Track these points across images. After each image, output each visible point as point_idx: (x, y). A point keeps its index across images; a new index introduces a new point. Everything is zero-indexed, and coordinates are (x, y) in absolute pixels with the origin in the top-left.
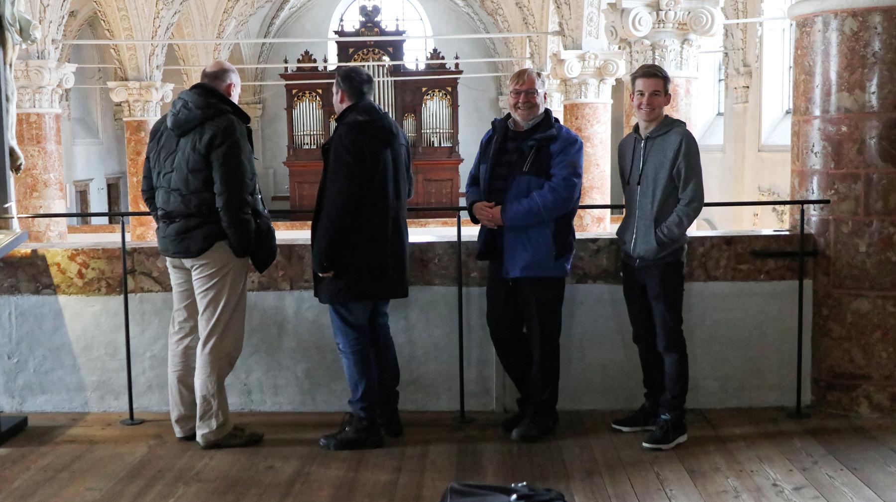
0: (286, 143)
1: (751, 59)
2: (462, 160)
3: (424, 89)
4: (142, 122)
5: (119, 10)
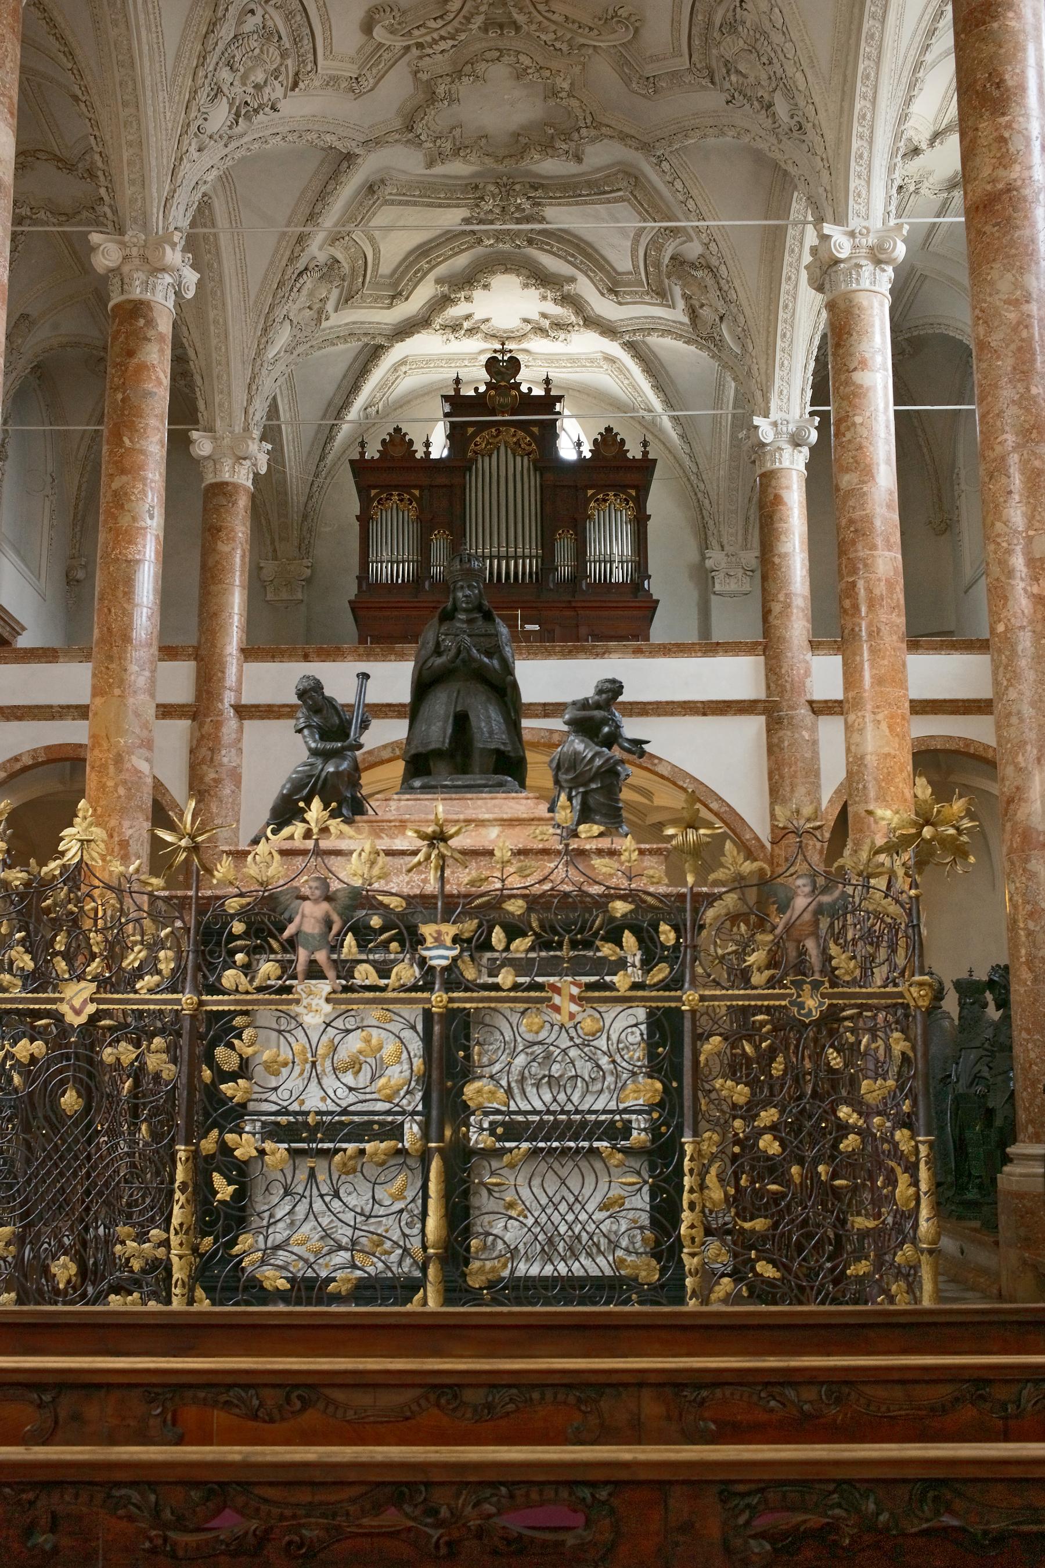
0: (356, 571)
2: (657, 601)
3: (590, 492)
4: (141, 302)
5: (125, 104)
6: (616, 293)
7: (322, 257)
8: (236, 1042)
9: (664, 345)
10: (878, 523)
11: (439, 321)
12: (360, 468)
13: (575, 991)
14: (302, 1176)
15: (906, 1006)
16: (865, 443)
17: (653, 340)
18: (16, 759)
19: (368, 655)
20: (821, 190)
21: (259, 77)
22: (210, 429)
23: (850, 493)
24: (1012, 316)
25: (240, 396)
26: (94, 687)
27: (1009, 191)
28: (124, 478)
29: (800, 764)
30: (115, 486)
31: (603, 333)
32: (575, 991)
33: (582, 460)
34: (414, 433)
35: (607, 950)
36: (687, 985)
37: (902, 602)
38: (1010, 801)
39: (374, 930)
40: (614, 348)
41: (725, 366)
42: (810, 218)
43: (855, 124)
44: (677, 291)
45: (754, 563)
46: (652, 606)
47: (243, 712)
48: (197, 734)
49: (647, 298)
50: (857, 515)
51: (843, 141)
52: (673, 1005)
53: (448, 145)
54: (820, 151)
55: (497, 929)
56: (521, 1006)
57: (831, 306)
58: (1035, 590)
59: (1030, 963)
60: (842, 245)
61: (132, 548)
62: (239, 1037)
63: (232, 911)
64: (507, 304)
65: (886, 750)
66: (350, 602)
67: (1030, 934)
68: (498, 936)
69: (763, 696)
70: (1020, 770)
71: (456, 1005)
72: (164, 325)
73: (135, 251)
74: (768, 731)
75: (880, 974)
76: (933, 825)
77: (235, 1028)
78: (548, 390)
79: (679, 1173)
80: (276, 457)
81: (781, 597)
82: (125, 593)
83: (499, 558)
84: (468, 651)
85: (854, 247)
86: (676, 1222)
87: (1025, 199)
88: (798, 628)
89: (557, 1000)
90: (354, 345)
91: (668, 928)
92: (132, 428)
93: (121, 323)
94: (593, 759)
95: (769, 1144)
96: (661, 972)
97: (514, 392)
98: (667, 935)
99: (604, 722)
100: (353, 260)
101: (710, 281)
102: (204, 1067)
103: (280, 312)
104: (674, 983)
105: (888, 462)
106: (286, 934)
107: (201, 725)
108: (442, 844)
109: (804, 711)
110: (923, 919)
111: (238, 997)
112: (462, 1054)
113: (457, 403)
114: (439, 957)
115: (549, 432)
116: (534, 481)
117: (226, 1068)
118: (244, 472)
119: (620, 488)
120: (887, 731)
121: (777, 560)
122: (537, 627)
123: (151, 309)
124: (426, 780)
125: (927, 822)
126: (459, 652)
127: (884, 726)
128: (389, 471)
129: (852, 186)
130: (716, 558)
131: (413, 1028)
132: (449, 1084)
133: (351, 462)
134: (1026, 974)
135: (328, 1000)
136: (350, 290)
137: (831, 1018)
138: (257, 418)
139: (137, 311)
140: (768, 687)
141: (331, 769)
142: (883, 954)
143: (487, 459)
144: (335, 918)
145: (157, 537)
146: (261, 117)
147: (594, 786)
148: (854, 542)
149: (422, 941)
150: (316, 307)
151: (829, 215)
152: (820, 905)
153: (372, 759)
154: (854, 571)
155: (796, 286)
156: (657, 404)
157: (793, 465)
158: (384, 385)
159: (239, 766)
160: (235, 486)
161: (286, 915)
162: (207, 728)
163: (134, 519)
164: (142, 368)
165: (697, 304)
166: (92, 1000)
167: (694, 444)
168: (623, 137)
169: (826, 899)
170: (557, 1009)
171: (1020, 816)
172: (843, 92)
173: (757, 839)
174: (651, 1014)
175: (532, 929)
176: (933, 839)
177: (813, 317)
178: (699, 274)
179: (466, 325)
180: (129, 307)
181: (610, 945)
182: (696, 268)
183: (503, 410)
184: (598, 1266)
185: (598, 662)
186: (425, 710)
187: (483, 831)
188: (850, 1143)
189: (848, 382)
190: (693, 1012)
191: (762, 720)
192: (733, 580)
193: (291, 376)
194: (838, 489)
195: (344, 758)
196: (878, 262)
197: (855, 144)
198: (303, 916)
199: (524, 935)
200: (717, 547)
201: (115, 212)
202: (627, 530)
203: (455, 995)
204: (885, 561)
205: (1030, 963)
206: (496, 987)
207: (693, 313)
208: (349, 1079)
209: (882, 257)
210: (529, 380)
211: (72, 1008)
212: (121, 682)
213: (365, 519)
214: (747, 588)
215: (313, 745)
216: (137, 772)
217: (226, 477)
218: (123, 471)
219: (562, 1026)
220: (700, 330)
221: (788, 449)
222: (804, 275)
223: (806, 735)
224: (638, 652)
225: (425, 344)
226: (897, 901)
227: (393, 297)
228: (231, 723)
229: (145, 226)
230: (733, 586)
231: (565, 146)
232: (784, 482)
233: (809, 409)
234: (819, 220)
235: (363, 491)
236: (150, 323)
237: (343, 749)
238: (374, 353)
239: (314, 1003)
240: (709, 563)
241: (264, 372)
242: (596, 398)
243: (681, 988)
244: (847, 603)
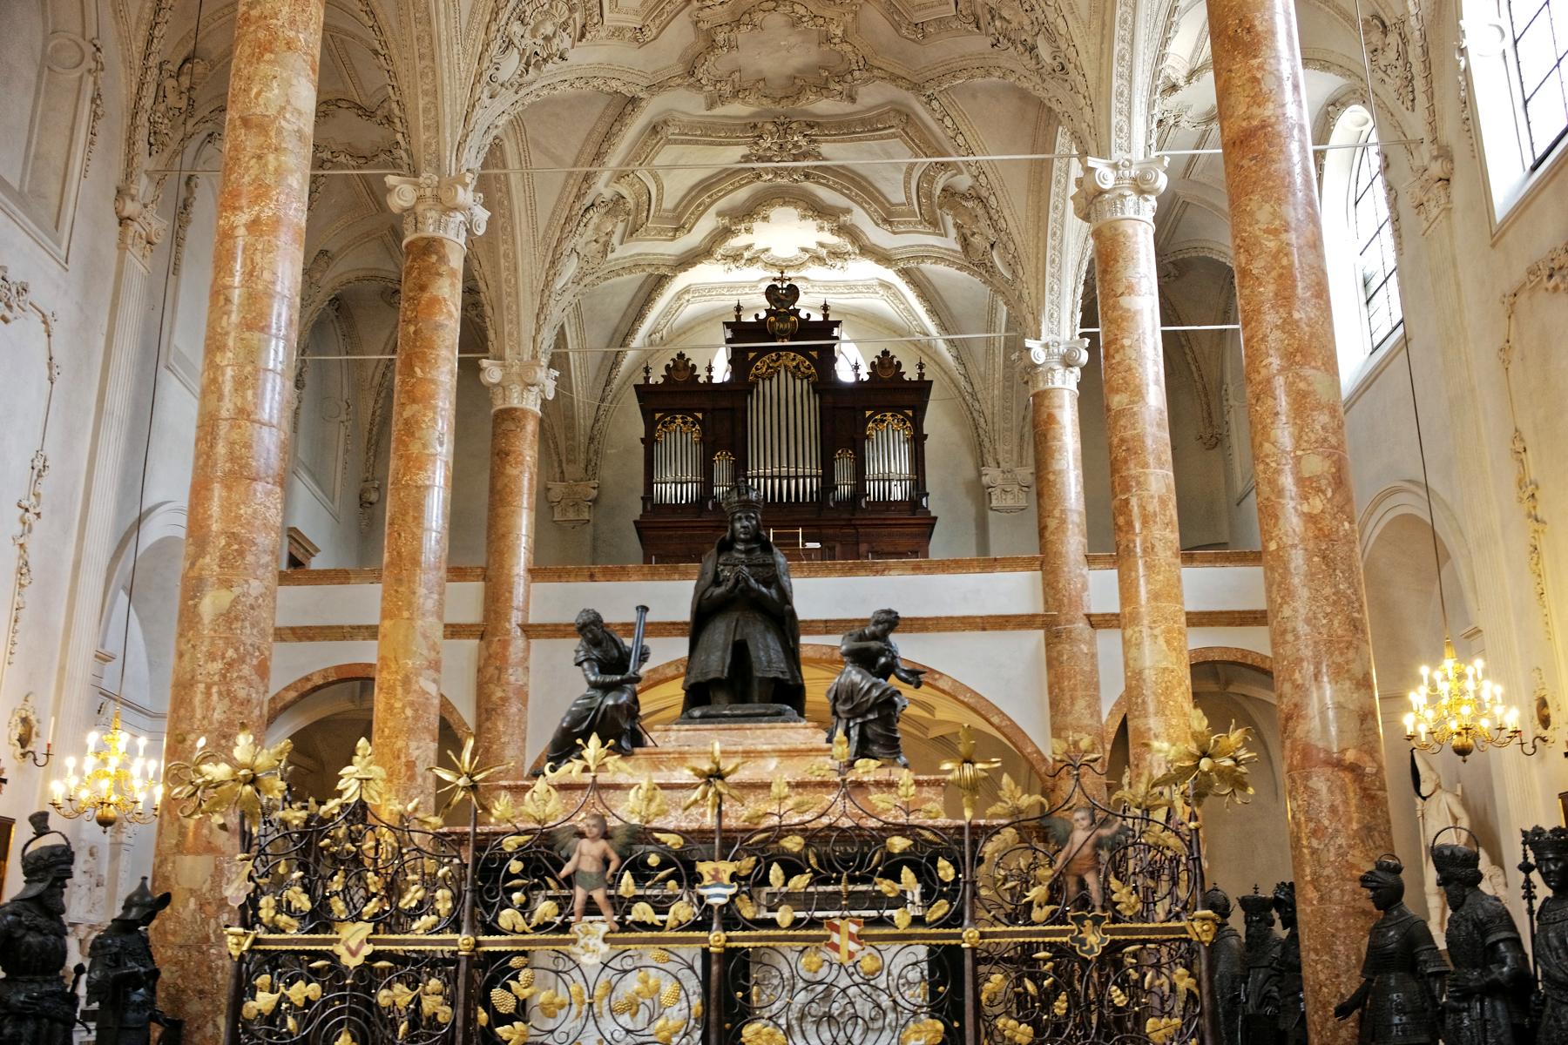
1: (1449, 131)
2: (935, 518)
3: (868, 413)
4: (434, 240)
5: (422, 57)
6: (891, 223)
7: (608, 194)
8: (512, 983)
9: (937, 271)
10: (1149, 441)
11: (720, 251)
12: (645, 393)
13: (854, 929)
15: (1189, 941)
16: (1134, 365)
17: (928, 267)
18: (307, 679)
19: (653, 575)
20: (1084, 125)
21: (548, 29)
22: (500, 357)
23: (1121, 413)
24: (1271, 244)
25: (528, 325)
26: (383, 610)
27: (1263, 127)
28: (415, 407)
29: (1079, 677)
30: (406, 414)
31: (878, 261)
32: (854, 929)
33: (859, 383)
34: (697, 358)
35: (885, 886)
36: (966, 922)
37: (1175, 518)
38: (1289, 718)
39: (652, 868)
40: (890, 275)
41: (997, 291)
42: (1075, 152)
43: (1115, 65)
44: (949, 220)
45: (1030, 479)
47: (529, 631)
48: (485, 654)
49: (920, 228)
50: (1129, 434)
51: (1104, 79)
52: (953, 942)
53: (728, 88)
54: (1082, 90)
55: (775, 866)
56: (800, 945)
57: (1097, 234)
58: (1306, 508)
59: (1315, 882)
60: (1106, 177)
61: (422, 475)
62: (515, 978)
63: (509, 850)
64: (785, 235)
65: (1164, 664)
66: (635, 522)
67: (1314, 852)
68: (776, 872)
69: (1040, 610)
70: (1297, 687)
71: (734, 945)
72: (456, 261)
73: (428, 192)
74: (1047, 645)
75: (1161, 910)
76: (1210, 756)
77: (512, 969)
78: (826, 316)
80: (563, 383)
81: (1057, 513)
82: (415, 518)
83: (780, 478)
84: (746, 581)
85: (1118, 179)
87: (1279, 135)
88: (1073, 542)
89: (836, 938)
90: (639, 276)
91: (946, 863)
92: (424, 360)
93: (414, 260)
94: (869, 690)
96: (941, 908)
97: (793, 319)
98: (945, 870)
99: (881, 652)
100: (638, 196)
101: (980, 211)
102: (480, 1009)
103: (567, 246)
104: (955, 919)
105: (1157, 382)
106: (564, 873)
107: (489, 645)
108: (719, 782)
109: (1081, 625)
110: (1203, 852)
111: (515, 937)
112: (740, 994)
113: (739, 330)
114: (717, 895)
115: (827, 357)
116: (813, 403)
117: (502, 1010)
118: (532, 398)
119: (897, 409)
120: (1164, 647)
121: (1051, 477)
122: (817, 545)
123: (443, 246)
124: (705, 709)
125: (1205, 754)
126: (737, 581)
127: (1161, 640)
128: (673, 395)
129: (1114, 122)
130: (992, 475)
131: (691, 968)
132: (728, 1026)
133: (636, 386)
134: (1312, 894)
135: (605, 940)
136: (635, 223)
138: (545, 346)
139: (430, 248)
140: (1046, 602)
141: (610, 702)
142: (1164, 887)
143: (767, 383)
144: (613, 856)
145: (447, 463)
146: (550, 65)
147: (871, 717)
148: (1126, 461)
149: (698, 878)
150: (602, 240)
151: (1092, 147)
152: (1100, 839)
153: (656, 677)
154: (1127, 489)
155: (1063, 215)
157: (1065, 384)
159: (526, 684)
160: (524, 412)
161: (563, 853)
162: (495, 647)
163: (425, 446)
164: (435, 301)
165: (968, 233)
166: (368, 941)
167: (969, 366)
168: (894, 78)
169: (1105, 832)
170: (836, 948)
171: (1300, 733)
172: (1103, 36)
173: (1038, 752)
174: (931, 952)
175: (810, 866)
176: (1211, 770)
177: (1080, 244)
178: (970, 204)
179: (747, 255)
180: (422, 244)
181: (889, 881)
182: (967, 199)
183: (782, 334)
185: (878, 578)
186: (705, 639)
187: (761, 762)
189: (1115, 307)
190: (974, 949)
191: (1041, 633)
192: (1009, 496)
193: (578, 306)
194: (1109, 410)
195: (623, 691)
196: (1141, 192)
197: (1116, 83)
198: (581, 854)
199: (803, 872)
200: (993, 464)
201: (410, 155)
202: (905, 449)
203: (733, 934)
204: (1156, 480)
205: (1315, 882)
206: (772, 924)
207: (965, 242)
208: (625, 1019)
209: (1145, 187)
210: (808, 307)
211: (349, 949)
212: (410, 605)
213: (649, 442)
214: (1023, 503)
215: (593, 678)
216: (425, 693)
217: (515, 402)
219: (841, 965)
220: (972, 258)
221: (1059, 370)
222: (1070, 205)
223: (1085, 648)
224: (917, 569)
225: (706, 273)
226: (1177, 834)
227: (676, 230)
228: (518, 642)
230: (1009, 502)
231: (838, 88)
232: (1056, 401)
233: (1079, 331)
234: (1084, 154)
235: (647, 414)
236: (442, 259)
237: (623, 682)
238: (659, 282)
239: (591, 943)
240: (985, 480)
241: (552, 302)
242: (871, 321)
243: (961, 925)
244: (1121, 520)
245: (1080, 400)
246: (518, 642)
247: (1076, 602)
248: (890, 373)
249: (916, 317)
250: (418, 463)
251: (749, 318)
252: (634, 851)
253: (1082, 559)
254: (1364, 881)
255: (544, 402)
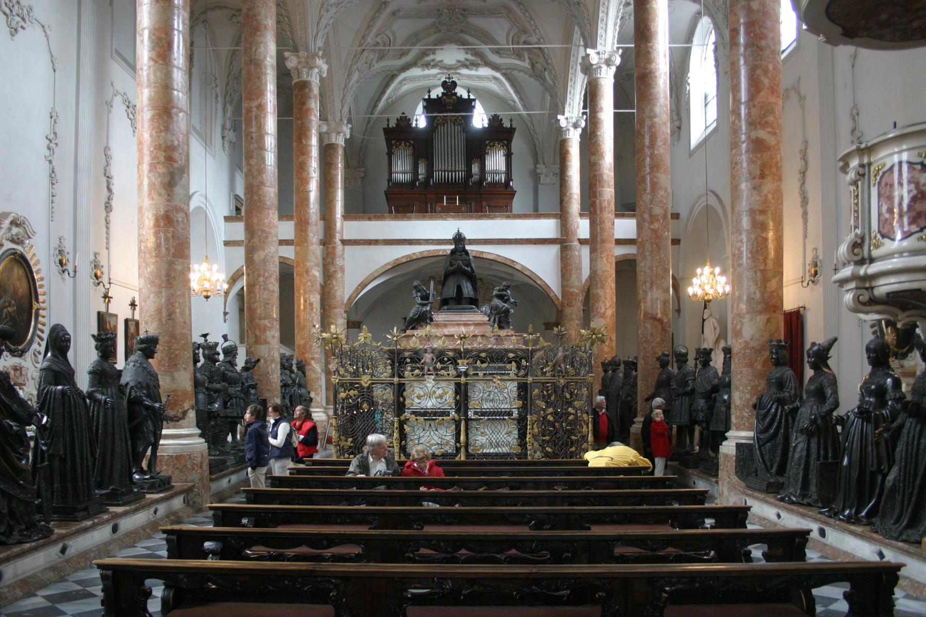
0: (387, 177)
12: (387, 131)
14: (428, 425)
24: (649, 123)
25: (338, 105)
30: (300, 160)
33: (484, 128)
40: (498, 75)
42: (582, 43)
45: (558, 171)
46: (513, 194)
47: (345, 242)
60: (594, 59)
64: (450, 55)
68: (478, 362)
72: (316, 91)
73: (303, 60)
79: (526, 425)
86: (525, 437)
88: (575, 206)
95: (550, 418)
96: (522, 372)
98: (524, 362)
101: (541, 55)
104: (526, 375)
109: (576, 243)
114: (462, 368)
119: (500, 140)
129: (599, 32)
133: (384, 129)
137: (567, 385)
151: (589, 44)
156: (517, 100)
157: (574, 138)
158: (395, 90)
160: (337, 145)
162: (330, 250)
164: (309, 110)
183: (449, 106)
184: (505, 450)
186: (447, 283)
188: (571, 417)
197: (601, 15)
201: (294, 41)
204: (608, 192)
205: (644, 358)
208: (439, 400)
213: (390, 155)
216: (315, 276)
217: (334, 141)
218: (303, 154)
220: (537, 73)
221: (572, 129)
222: (579, 68)
224: (508, 217)
228: (340, 247)
229: (307, 49)
230: (548, 180)
232: (570, 144)
233: (582, 111)
235: (388, 141)
236: (311, 90)
238: (393, 77)
240: (538, 171)
242: (488, 97)
245: (581, 143)
246: (340, 247)
247: (574, 233)
248: (498, 123)
249: (509, 93)
250: (305, 181)
251: (433, 96)
252: (440, 355)
253: (577, 215)
254: (658, 359)
255: (346, 141)
